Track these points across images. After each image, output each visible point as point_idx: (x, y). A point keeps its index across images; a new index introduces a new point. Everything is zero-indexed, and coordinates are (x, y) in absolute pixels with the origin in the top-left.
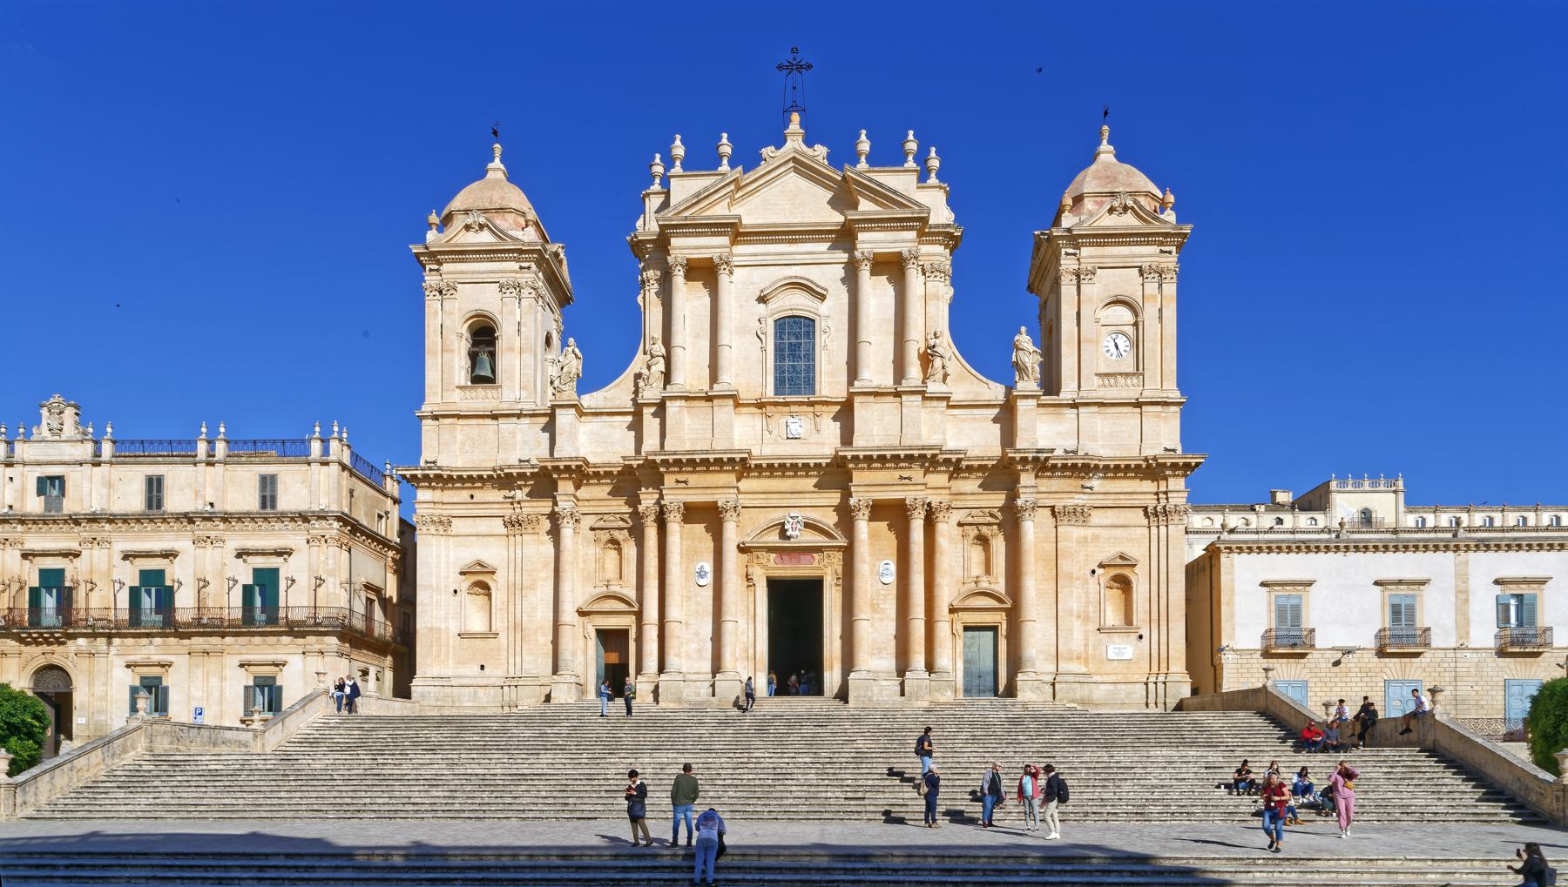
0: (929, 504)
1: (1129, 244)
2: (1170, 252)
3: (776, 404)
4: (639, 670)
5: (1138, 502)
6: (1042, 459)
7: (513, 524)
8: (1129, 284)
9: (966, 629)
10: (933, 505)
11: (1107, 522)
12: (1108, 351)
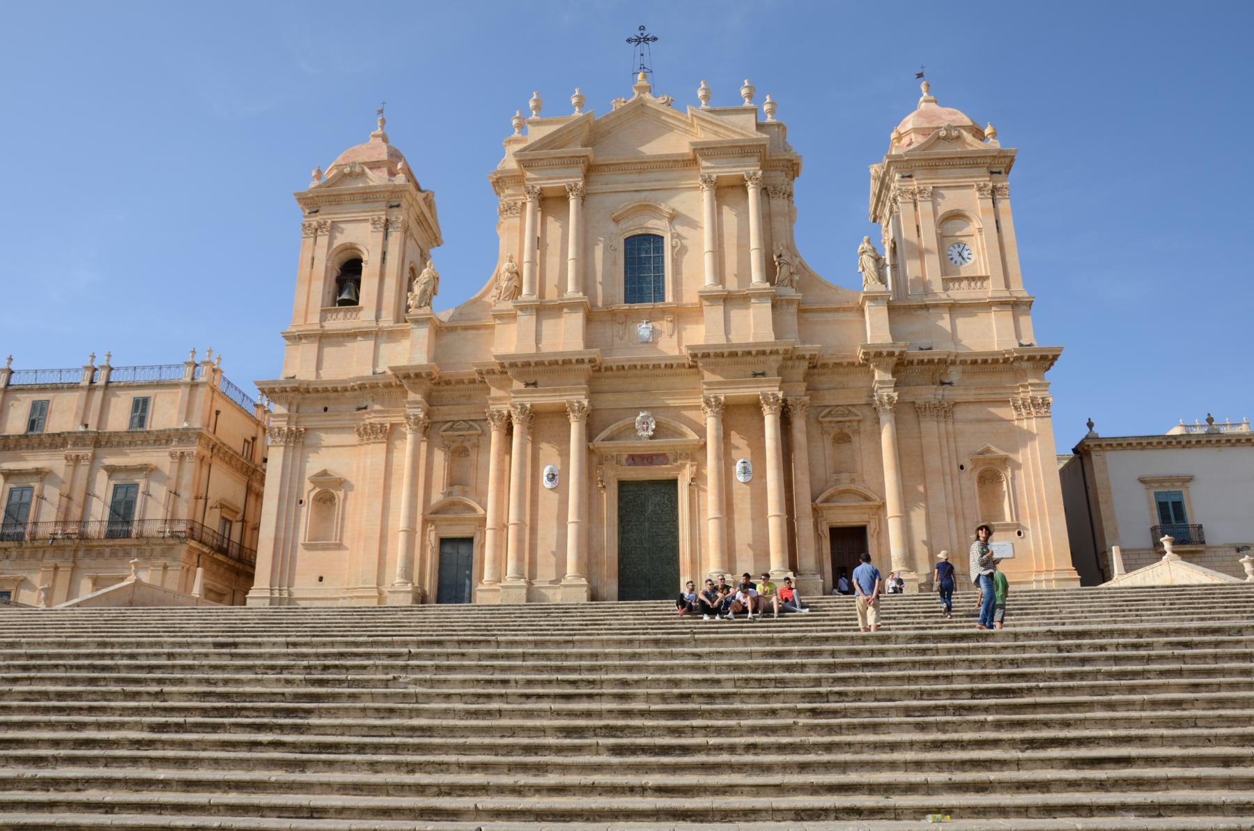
0: (784, 401)
4: (481, 577)
5: (999, 396)
6: (897, 353)
10: (789, 403)
11: (970, 416)
12: (952, 259)
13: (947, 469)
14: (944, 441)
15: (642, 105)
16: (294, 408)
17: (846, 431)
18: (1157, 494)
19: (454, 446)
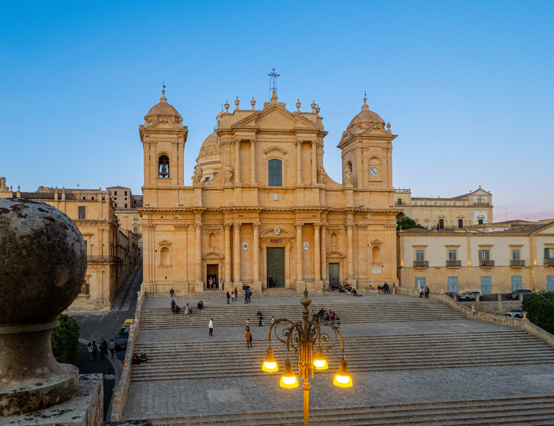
1: (378, 140)
3: (270, 189)
7: (178, 227)
8: (378, 152)
9: (330, 264)
11: (372, 229)
14: (364, 237)
16: (150, 216)
17: (336, 232)
19: (210, 233)
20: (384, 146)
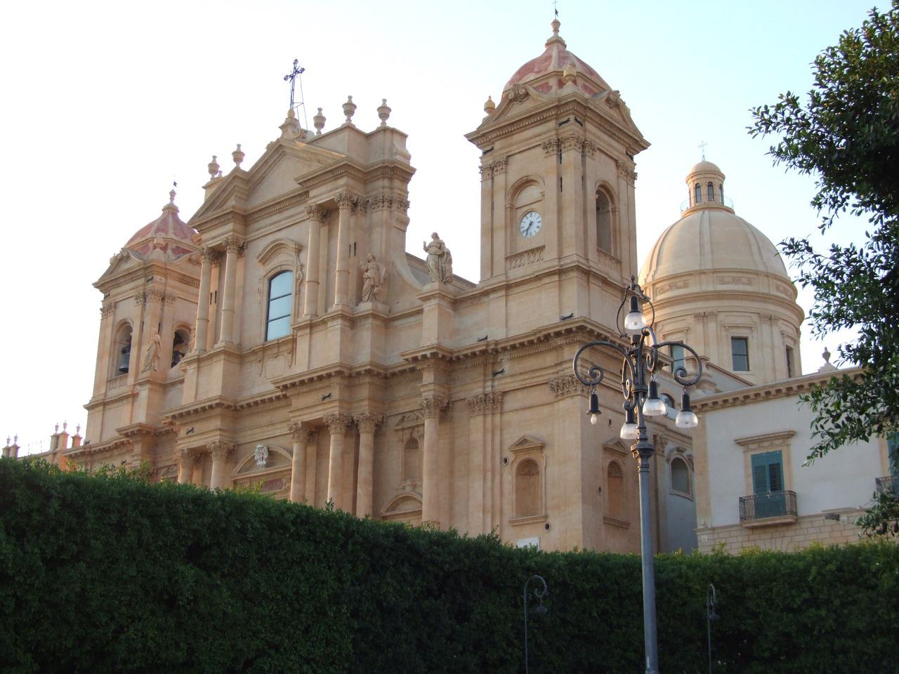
2: (568, 121)
5: (541, 379)
10: (355, 419)
11: (517, 405)
13: (489, 465)
14: (489, 437)
15: (280, 145)
18: (754, 457)
20: (544, 139)
